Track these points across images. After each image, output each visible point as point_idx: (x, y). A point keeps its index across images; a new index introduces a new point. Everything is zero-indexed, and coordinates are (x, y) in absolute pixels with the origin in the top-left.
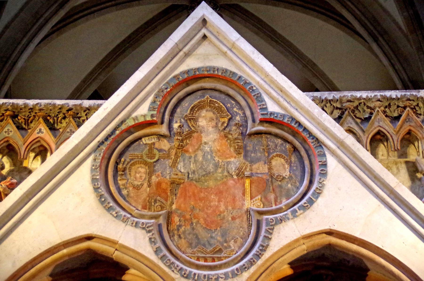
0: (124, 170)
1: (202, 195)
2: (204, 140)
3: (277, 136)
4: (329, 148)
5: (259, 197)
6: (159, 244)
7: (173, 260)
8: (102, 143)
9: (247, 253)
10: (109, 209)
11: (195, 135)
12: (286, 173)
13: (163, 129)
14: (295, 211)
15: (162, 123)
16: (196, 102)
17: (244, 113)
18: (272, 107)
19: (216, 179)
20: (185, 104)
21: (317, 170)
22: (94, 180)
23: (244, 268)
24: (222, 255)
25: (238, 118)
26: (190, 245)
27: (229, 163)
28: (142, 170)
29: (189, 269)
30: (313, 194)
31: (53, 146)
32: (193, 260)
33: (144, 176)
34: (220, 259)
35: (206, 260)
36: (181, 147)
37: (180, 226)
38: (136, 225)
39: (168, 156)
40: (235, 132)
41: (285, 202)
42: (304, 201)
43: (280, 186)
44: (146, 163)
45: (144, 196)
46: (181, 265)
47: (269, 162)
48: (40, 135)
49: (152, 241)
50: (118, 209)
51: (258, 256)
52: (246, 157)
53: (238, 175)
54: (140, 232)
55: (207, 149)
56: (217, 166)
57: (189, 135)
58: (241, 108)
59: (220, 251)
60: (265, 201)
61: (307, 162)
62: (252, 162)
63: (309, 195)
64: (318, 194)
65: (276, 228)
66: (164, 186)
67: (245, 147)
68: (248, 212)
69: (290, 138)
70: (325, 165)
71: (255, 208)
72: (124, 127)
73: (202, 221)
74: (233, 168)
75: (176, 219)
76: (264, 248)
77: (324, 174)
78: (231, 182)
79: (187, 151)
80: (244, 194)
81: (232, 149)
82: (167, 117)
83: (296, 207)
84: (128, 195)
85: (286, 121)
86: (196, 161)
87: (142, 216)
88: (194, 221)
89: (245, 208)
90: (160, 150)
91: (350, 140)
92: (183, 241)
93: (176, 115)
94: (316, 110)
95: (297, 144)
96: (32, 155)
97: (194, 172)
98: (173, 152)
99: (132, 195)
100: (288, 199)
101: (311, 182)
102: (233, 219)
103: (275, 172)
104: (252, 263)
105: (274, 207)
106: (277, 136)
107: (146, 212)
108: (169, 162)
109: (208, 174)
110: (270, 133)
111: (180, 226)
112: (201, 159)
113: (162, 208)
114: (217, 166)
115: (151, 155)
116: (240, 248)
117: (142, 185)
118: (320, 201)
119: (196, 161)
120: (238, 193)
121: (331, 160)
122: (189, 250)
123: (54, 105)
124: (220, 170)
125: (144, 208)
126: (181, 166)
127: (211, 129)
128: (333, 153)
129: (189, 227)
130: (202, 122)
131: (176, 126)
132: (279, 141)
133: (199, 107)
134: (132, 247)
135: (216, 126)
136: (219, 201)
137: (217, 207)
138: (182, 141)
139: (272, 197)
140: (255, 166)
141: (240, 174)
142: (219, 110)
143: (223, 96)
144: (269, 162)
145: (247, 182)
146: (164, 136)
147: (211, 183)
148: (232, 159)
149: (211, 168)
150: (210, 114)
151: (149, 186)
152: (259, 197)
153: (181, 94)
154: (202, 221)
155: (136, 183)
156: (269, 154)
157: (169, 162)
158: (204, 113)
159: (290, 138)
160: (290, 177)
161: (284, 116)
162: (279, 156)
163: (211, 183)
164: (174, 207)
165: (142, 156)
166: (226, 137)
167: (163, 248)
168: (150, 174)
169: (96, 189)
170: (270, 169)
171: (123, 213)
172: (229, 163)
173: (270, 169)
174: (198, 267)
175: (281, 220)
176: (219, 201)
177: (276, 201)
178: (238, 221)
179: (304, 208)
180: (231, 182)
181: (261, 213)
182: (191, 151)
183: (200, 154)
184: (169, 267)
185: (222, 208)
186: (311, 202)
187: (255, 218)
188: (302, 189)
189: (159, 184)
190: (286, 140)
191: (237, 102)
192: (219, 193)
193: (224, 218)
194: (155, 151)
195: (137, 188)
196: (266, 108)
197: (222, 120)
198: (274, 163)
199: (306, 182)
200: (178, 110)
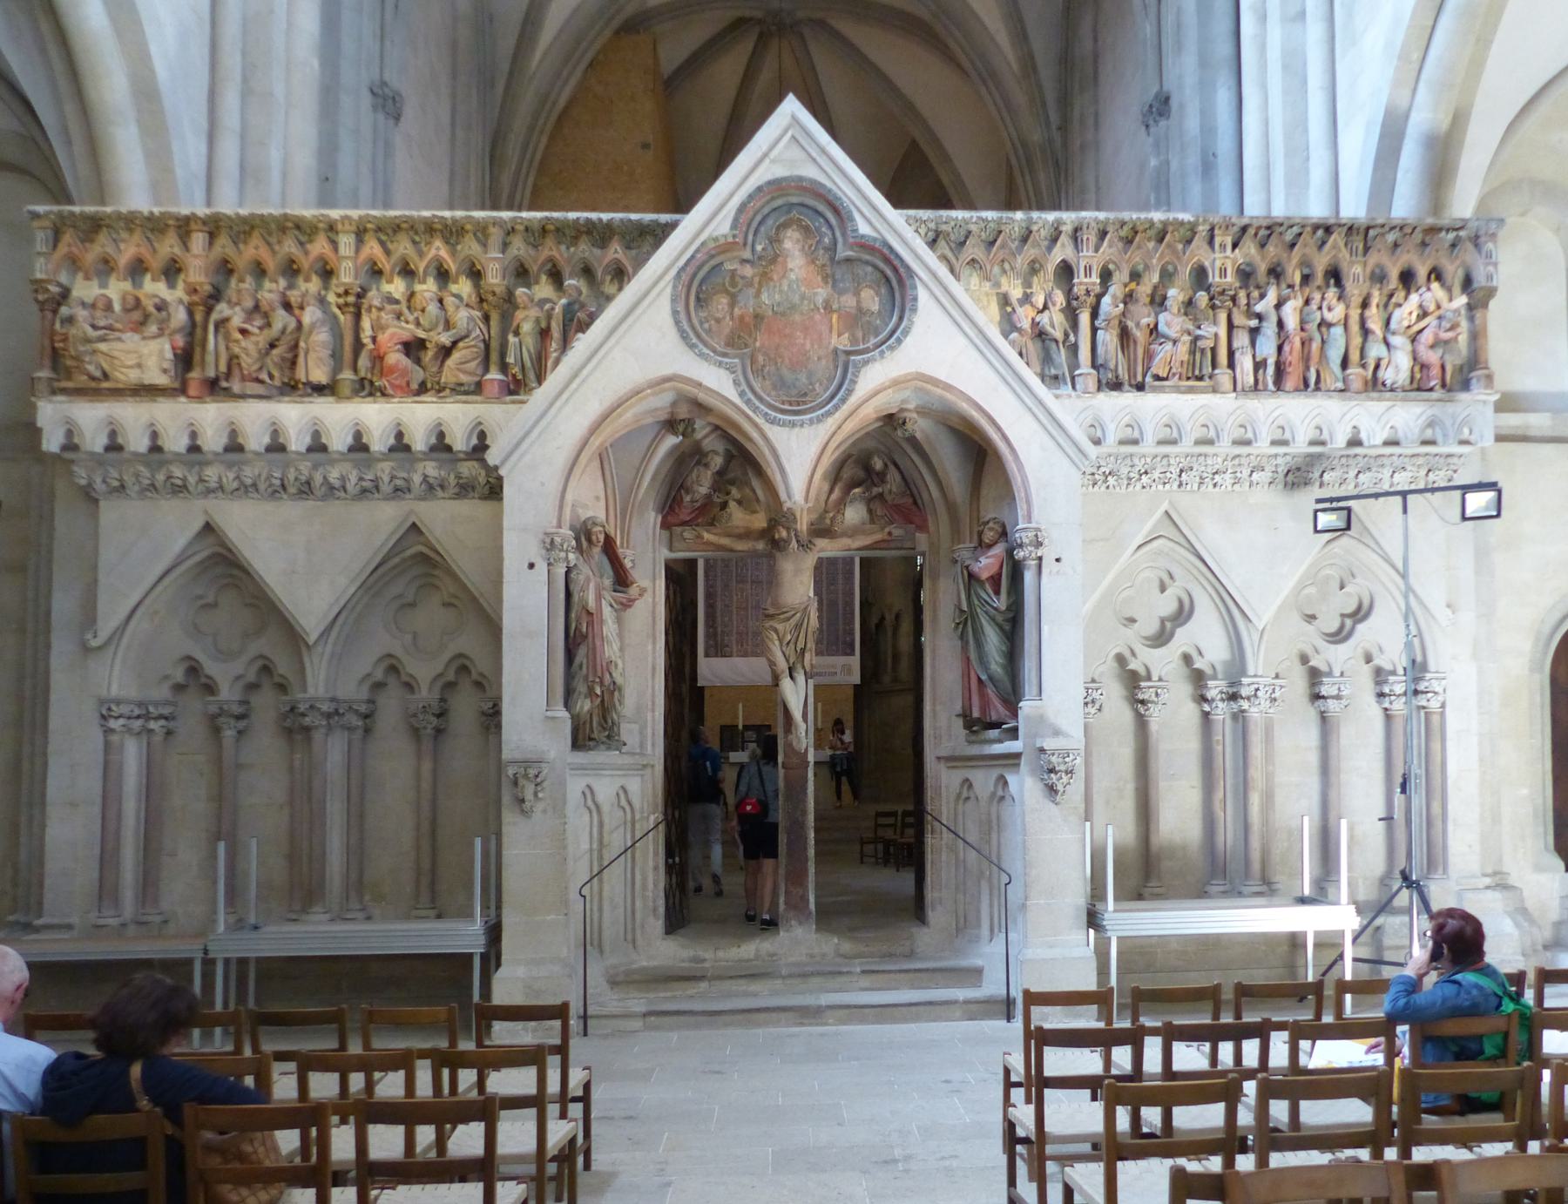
0: (705, 300)
1: (787, 331)
2: (790, 265)
3: (867, 263)
4: (920, 279)
5: (847, 335)
6: (744, 387)
7: (757, 403)
8: (683, 269)
9: (833, 397)
10: (692, 346)
11: (780, 259)
12: (875, 307)
13: (747, 254)
14: (882, 353)
15: (745, 244)
16: (782, 220)
17: (834, 234)
18: (864, 229)
19: (802, 314)
20: (770, 222)
21: (908, 306)
22: (675, 313)
23: (829, 414)
24: (808, 398)
25: (826, 240)
26: (775, 387)
27: (815, 294)
28: (724, 301)
29: (774, 414)
30: (902, 333)
31: (630, 270)
32: (777, 404)
33: (726, 307)
34: (805, 403)
35: (791, 405)
36: (765, 277)
37: (764, 366)
38: (720, 364)
39: (750, 284)
40: (823, 257)
41: (873, 341)
42: (892, 340)
43: (869, 322)
44: (727, 292)
45: (727, 331)
46: (766, 410)
47: (857, 294)
48: (616, 256)
49: (736, 383)
50: (701, 346)
51: (843, 401)
52: (834, 286)
53: (825, 309)
54: (723, 373)
55: (793, 276)
56: (803, 297)
57: (774, 260)
58: (830, 227)
59: (805, 394)
60: (854, 341)
61: (897, 295)
62: (841, 293)
63: (898, 334)
64: (906, 333)
65: (863, 371)
66: (747, 319)
67: (833, 276)
68: (836, 351)
69: (881, 265)
70: (915, 299)
71: (841, 347)
72: (705, 250)
73: (787, 361)
74: (820, 300)
75: (761, 358)
76: (850, 392)
77: (914, 310)
78: (817, 317)
79: (771, 279)
80: (831, 332)
81: (819, 278)
82: (750, 237)
83: (884, 347)
84: (710, 330)
85: (877, 245)
86: (781, 292)
87: (725, 355)
88: (779, 360)
89: (832, 347)
90: (743, 278)
91: (943, 271)
92: (767, 382)
93: (759, 235)
94: (909, 233)
95: (889, 272)
96: (608, 278)
97: (779, 304)
98: (757, 279)
99: (714, 329)
100: (876, 336)
101: (901, 318)
102: (819, 359)
103: (865, 305)
104: (837, 408)
105: (862, 347)
106: (867, 263)
107: (729, 350)
108: (751, 291)
109: (793, 307)
110: (860, 260)
111: (764, 366)
112: (786, 288)
113: (746, 346)
114: (803, 297)
115: (734, 284)
116: (825, 391)
117: (724, 318)
118: (908, 340)
119: (781, 292)
120: (824, 328)
121: (922, 294)
122: (773, 393)
123: (630, 220)
124: (806, 302)
125: (728, 345)
126: (764, 297)
127: (797, 253)
128: (926, 286)
129: (773, 368)
130: (788, 244)
131: (759, 248)
132: (869, 269)
133: (784, 226)
134: (715, 388)
135: (803, 249)
136: (805, 338)
137: (803, 345)
138: (766, 267)
139: (860, 334)
140: (843, 299)
141: (828, 306)
142: (806, 230)
143: (810, 212)
144: (857, 294)
145: (835, 317)
146: (747, 261)
147: (797, 318)
148: (820, 290)
149: (796, 299)
150: (796, 235)
151: (732, 318)
152: (847, 335)
153: (766, 210)
154: (787, 361)
155: (719, 315)
156: (859, 284)
157: (751, 291)
158: (789, 233)
159: (881, 265)
160: (879, 311)
161: (875, 239)
162: (870, 287)
163: (797, 318)
164: (758, 344)
165: (724, 284)
166: (813, 262)
167: (747, 390)
168: (732, 305)
169: (677, 323)
170: (858, 302)
171: (706, 351)
172: (815, 294)
173: (858, 302)
174: (783, 412)
175: (866, 362)
176: (805, 338)
177: (864, 339)
178: (824, 362)
179: (891, 348)
180: (817, 317)
181: (848, 353)
182: (775, 277)
183: (785, 283)
184: (754, 412)
185: (808, 346)
186: (899, 341)
187: (842, 358)
188: (891, 326)
189: (742, 318)
190: (876, 267)
191: (827, 221)
192: (806, 330)
193: (809, 358)
194: (737, 279)
195: (718, 321)
196: (857, 230)
197: (810, 242)
198: (863, 294)
199: (895, 319)
200: (762, 229)
